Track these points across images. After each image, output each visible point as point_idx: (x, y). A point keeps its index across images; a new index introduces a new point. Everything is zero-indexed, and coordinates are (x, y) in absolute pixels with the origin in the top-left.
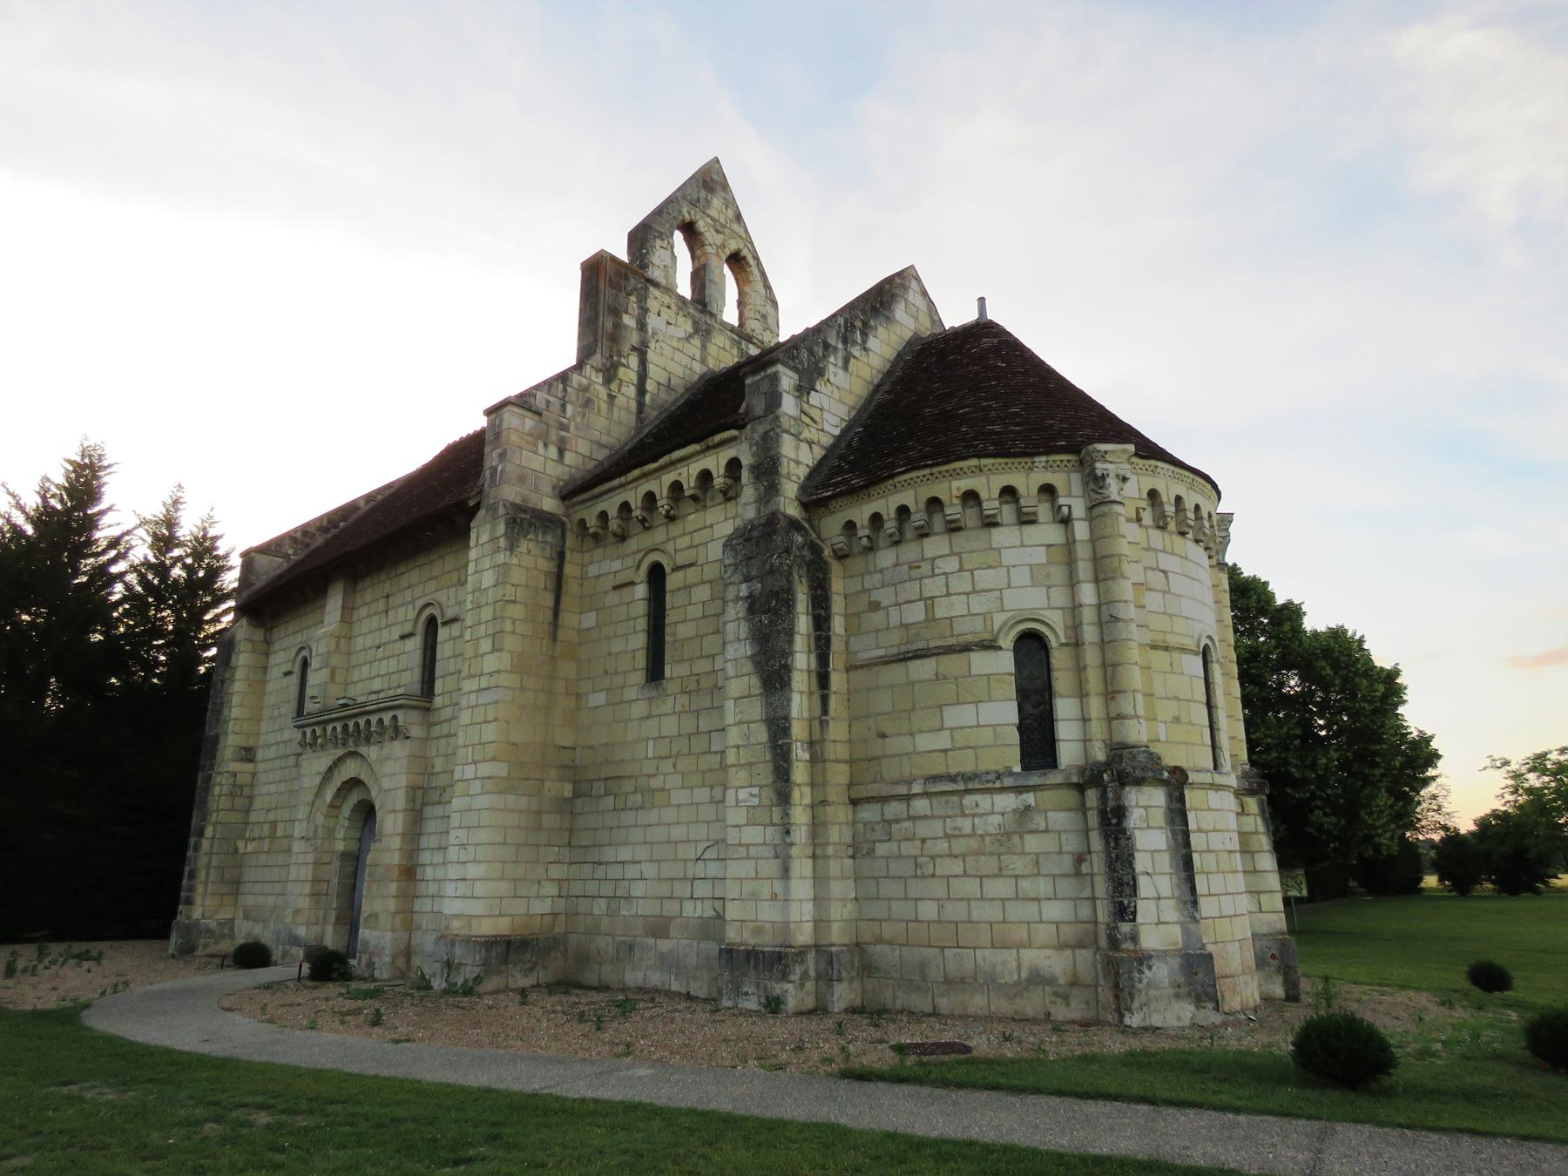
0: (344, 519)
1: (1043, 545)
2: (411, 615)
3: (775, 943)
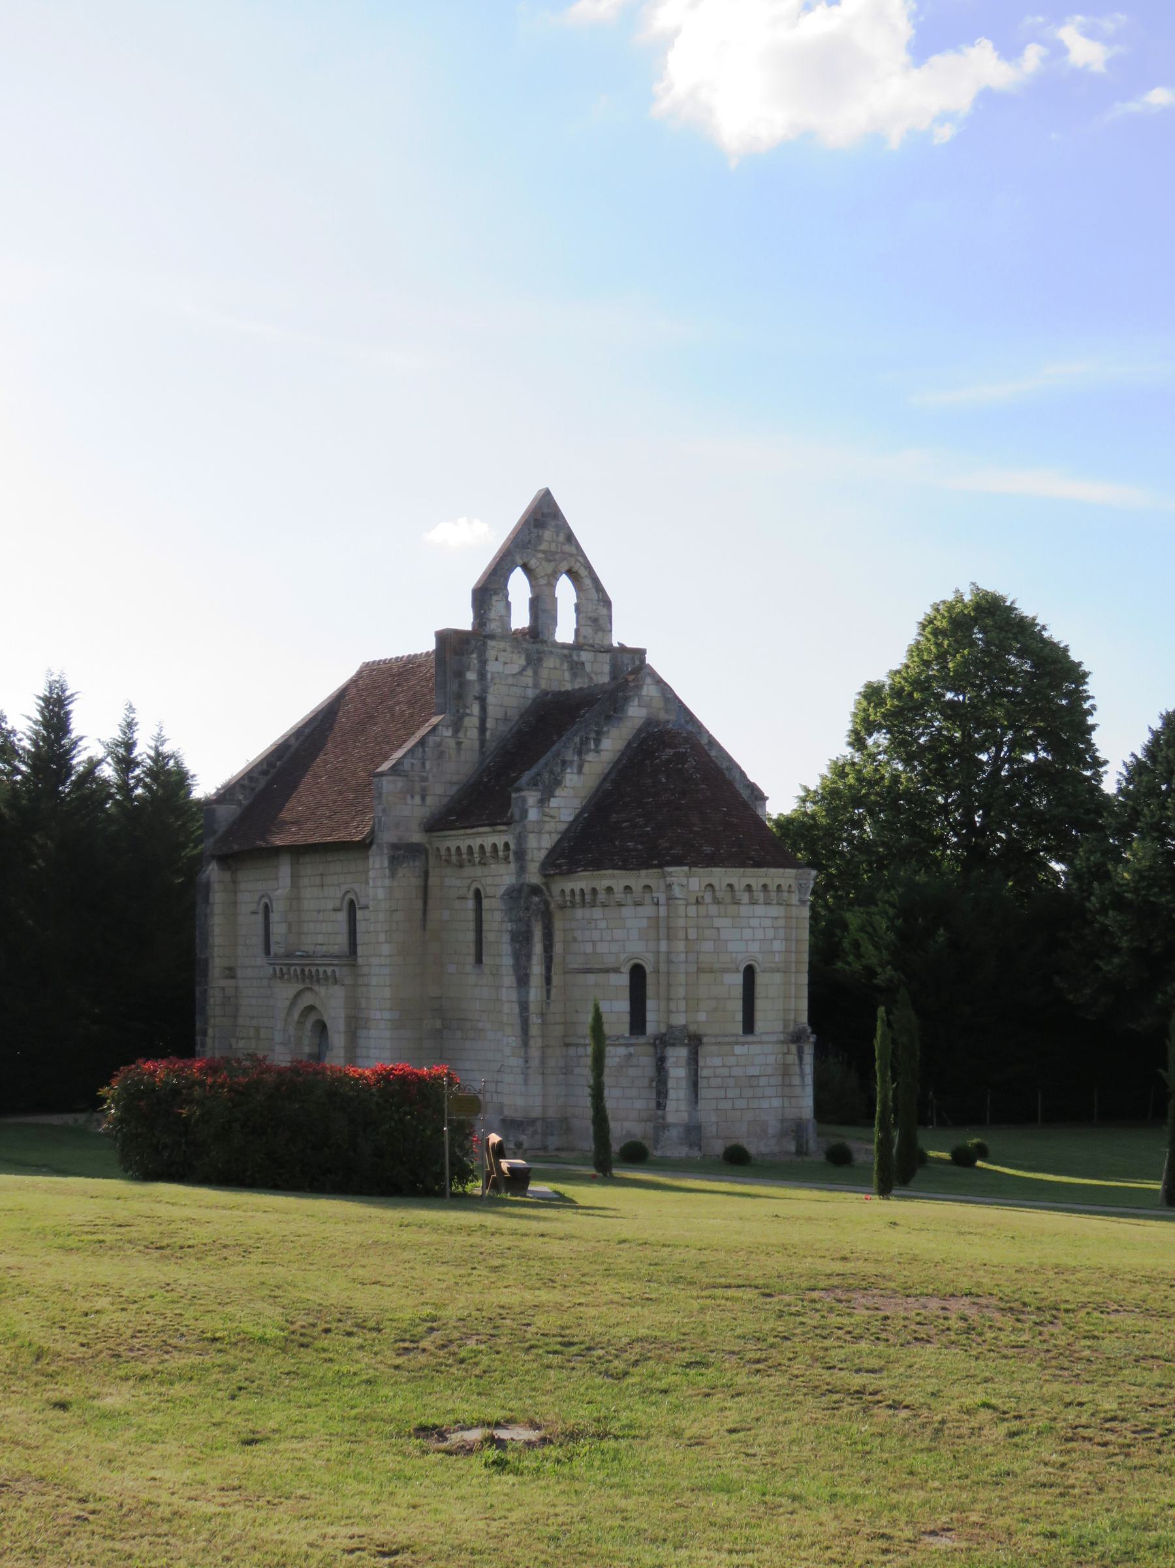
0: (279, 758)
2: (339, 895)
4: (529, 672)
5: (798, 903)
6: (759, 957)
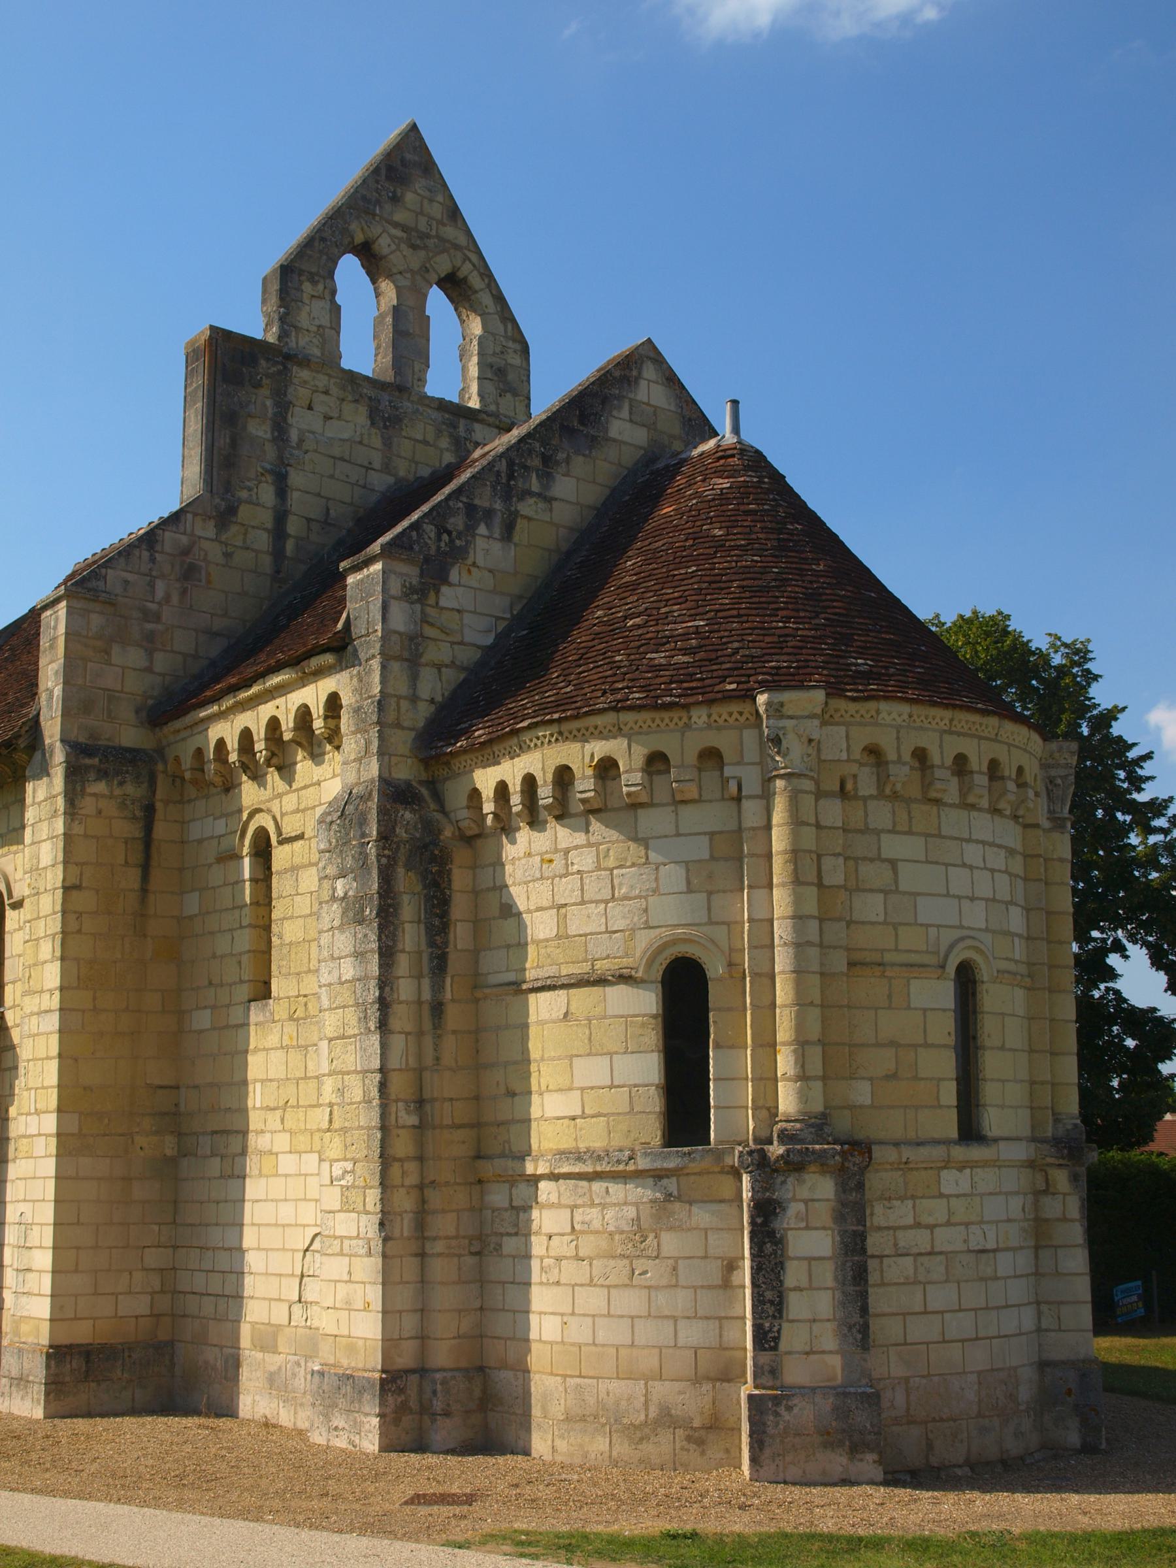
1: (705, 834)
3: (369, 1366)
5: (1046, 824)
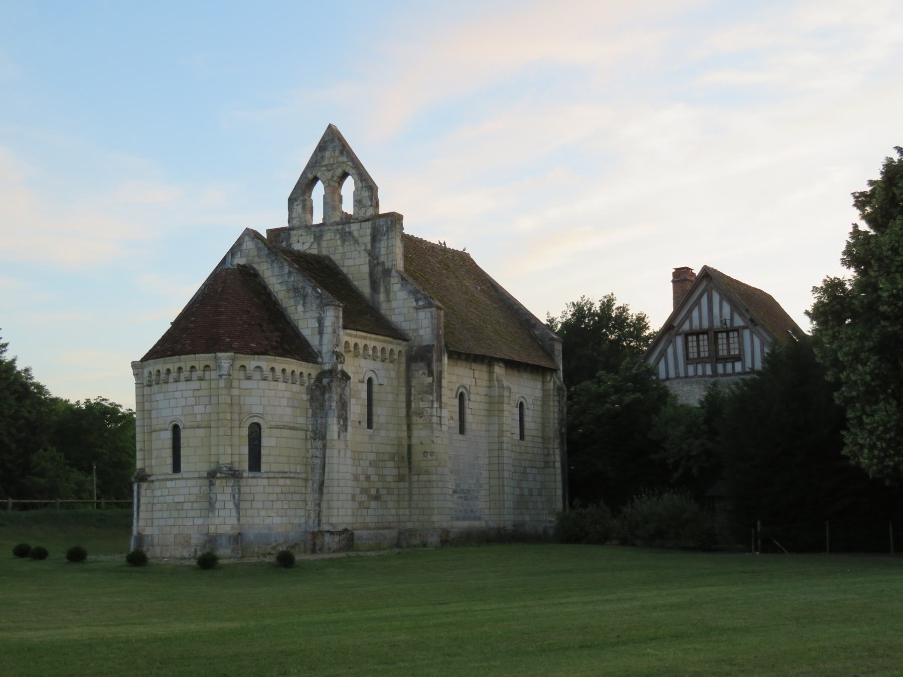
4: (315, 246)
6: (182, 418)
